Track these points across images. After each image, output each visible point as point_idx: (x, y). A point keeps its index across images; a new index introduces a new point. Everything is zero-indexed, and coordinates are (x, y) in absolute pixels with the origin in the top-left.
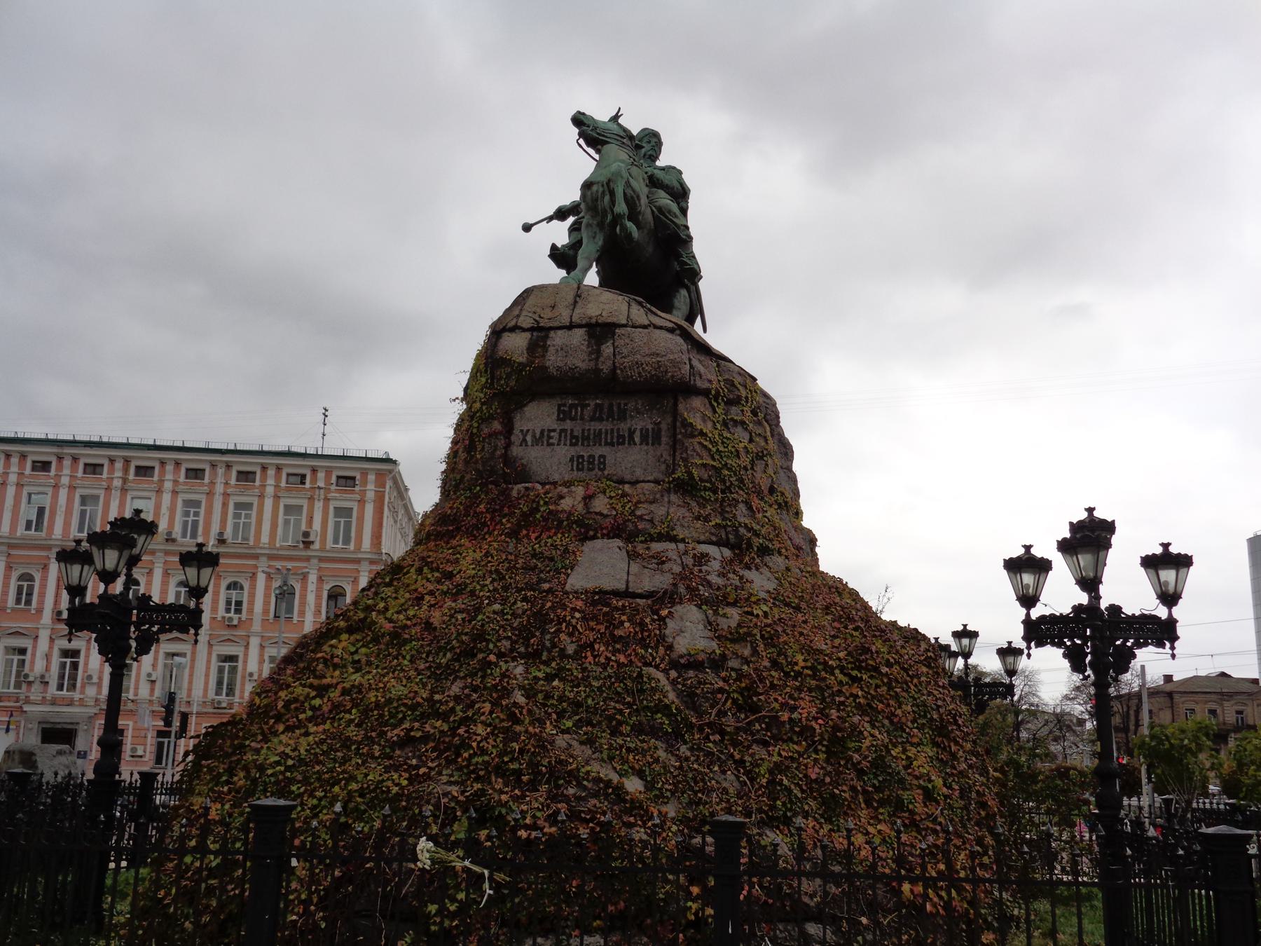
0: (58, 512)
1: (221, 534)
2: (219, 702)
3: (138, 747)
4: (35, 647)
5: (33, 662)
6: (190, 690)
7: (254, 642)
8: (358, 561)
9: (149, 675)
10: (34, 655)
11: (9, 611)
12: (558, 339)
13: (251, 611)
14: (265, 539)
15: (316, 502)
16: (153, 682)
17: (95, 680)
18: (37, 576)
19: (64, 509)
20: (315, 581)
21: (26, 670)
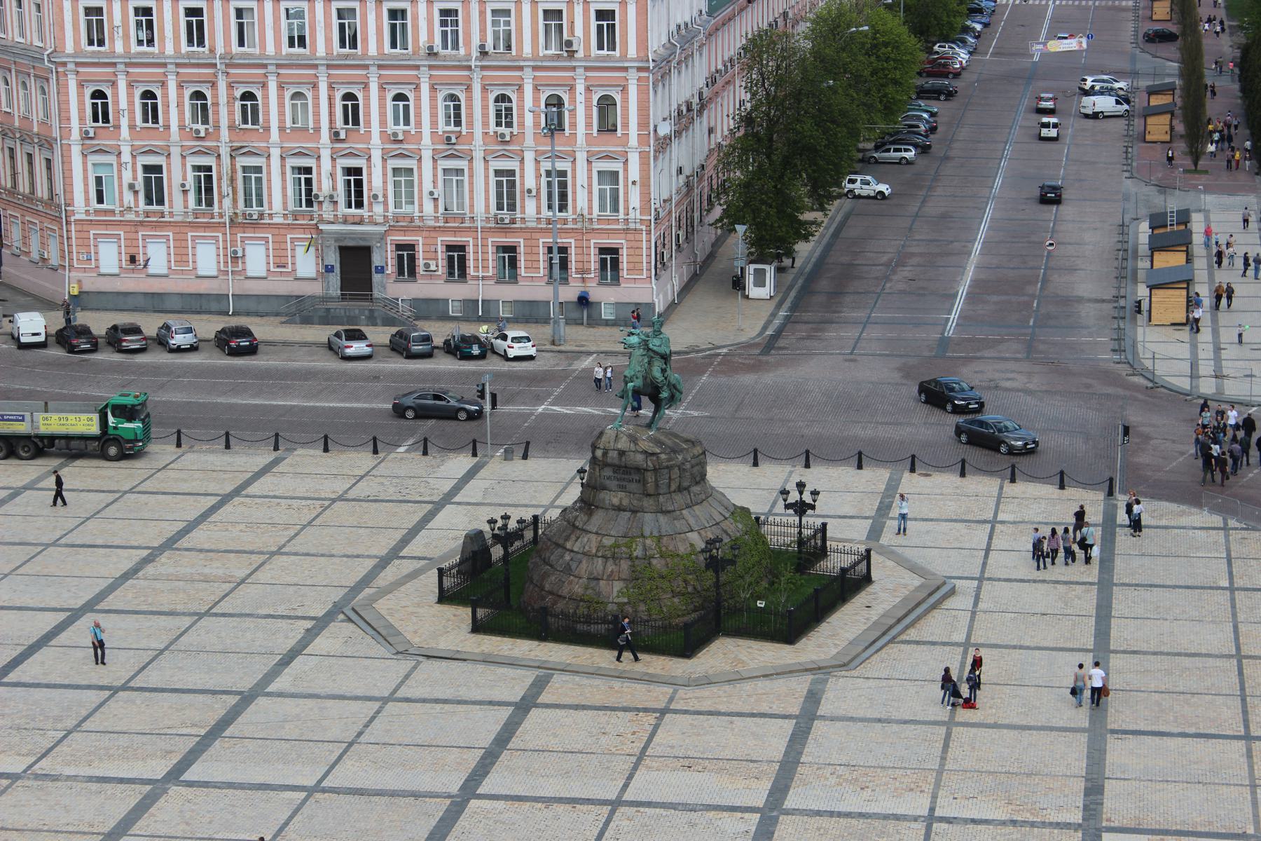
0: (318, 28)
1: (482, 46)
2: (502, 219)
3: (431, 262)
4: (319, 166)
5: (320, 181)
6: (472, 206)
7: (529, 156)
8: (625, 69)
9: (431, 193)
10: (319, 174)
11: (288, 131)
12: (611, 454)
13: (522, 124)
14: (527, 50)
15: (575, 4)
16: (436, 200)
17: (381, 199)
18: (309, 95)
19: (322, 24)
20: (583, 93)
21: (315, 191)
